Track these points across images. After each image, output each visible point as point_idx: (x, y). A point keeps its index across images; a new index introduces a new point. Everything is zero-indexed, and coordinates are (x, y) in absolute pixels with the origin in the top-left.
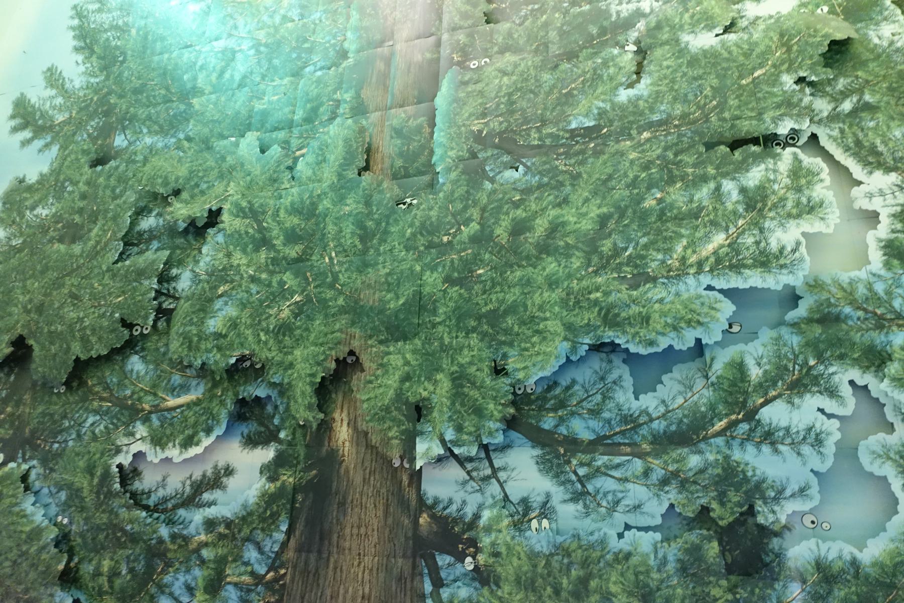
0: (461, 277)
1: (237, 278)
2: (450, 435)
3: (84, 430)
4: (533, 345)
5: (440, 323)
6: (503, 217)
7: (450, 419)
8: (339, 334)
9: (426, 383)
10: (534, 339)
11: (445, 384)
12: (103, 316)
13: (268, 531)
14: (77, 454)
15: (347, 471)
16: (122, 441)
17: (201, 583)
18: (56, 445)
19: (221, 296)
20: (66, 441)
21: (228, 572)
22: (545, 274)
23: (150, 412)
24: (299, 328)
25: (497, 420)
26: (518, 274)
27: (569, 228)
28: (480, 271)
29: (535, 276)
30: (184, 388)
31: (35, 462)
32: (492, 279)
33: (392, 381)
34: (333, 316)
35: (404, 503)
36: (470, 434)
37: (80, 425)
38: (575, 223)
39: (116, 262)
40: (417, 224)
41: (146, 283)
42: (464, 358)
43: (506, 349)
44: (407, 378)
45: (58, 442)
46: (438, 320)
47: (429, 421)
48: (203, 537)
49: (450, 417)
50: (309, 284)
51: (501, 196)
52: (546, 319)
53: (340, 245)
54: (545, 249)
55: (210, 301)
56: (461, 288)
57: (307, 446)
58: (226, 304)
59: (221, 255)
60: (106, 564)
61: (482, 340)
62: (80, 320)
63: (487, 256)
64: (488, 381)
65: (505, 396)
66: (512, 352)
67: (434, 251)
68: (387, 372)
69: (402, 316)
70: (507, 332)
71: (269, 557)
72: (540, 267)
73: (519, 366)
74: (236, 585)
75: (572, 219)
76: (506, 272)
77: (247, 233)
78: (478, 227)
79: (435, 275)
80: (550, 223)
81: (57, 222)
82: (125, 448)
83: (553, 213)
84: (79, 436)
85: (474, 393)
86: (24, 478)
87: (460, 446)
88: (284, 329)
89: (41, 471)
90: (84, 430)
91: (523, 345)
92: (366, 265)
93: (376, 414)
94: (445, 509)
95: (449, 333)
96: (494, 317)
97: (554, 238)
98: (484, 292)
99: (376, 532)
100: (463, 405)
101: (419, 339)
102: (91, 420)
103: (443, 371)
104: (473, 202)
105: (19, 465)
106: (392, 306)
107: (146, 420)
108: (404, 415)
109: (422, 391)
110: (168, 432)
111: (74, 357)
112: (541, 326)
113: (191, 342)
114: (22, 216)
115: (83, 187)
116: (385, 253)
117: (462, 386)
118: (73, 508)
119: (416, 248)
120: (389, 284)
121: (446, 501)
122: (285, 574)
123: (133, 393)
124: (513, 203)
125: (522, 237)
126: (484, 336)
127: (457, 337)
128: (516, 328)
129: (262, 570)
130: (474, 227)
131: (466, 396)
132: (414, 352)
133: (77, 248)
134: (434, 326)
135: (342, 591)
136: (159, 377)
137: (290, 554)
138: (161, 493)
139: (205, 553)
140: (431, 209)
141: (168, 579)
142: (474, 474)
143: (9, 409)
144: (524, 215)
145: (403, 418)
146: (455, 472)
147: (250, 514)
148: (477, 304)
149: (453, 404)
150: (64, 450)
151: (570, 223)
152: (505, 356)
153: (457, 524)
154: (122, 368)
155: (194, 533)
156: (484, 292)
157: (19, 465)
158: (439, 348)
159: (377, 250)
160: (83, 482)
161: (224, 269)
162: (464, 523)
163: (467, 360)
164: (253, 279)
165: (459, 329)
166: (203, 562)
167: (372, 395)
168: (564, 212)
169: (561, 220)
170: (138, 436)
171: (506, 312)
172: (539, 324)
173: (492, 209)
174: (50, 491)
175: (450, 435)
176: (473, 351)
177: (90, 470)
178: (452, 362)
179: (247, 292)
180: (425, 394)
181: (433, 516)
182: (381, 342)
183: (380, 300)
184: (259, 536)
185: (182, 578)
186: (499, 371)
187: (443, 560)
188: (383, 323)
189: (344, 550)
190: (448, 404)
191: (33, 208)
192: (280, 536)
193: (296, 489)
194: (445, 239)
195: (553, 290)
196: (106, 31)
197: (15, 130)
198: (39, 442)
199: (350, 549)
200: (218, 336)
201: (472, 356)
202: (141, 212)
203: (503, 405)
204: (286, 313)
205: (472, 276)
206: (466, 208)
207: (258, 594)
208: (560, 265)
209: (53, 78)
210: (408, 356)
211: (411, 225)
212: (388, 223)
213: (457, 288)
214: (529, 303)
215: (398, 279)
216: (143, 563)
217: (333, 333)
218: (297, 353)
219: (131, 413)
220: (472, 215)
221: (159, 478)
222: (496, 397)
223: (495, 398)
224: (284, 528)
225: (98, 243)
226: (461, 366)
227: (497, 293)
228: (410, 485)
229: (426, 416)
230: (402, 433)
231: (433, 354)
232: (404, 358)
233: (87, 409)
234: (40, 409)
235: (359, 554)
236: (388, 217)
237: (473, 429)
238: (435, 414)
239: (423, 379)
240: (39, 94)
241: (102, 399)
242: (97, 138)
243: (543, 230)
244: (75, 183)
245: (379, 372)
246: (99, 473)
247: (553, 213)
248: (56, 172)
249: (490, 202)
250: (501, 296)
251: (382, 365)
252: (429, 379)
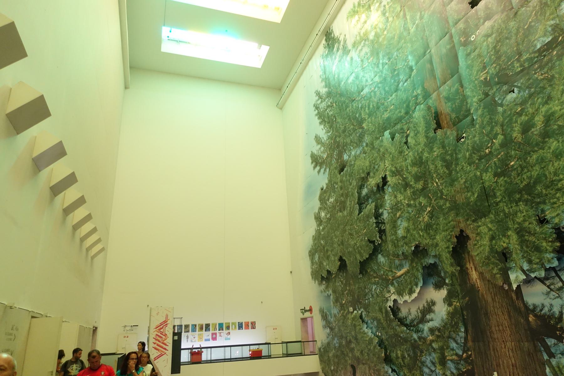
0: (503, 171)
1: (402, 207)
2: (526, 267)
4: (558, 199)
5: (500, 202)
6: (514, 125)
7: (523, 257)
8: (452, 223)
9: (503, 239)
10: (558, 195)
11: (514, 237)
12: (362, 240)
13: (457, 331)
14: (374, 304)
15: (483, 295)
16: (387, 295)
19: (399, 218)
21: (446, 354)
22: (551, 151)
23: (393, 280)
24: (434, 224)
25: (550, 252)
26: (535, 157)
27: (557, 115)
28: (512, 163)
29: (545, 155)
30: (401, 266)
31: (362, 310)
32: (521, 166)
33: (486, 241)
34: (447, 213)
35: (517, 310)
36: (537, 264)
38: (560, 110)
39: (359, 214)
40: (470, 148)
41: (371, 220)
42: (520, 219)
43: (542, 206)
44: (492, 238)
46: (498, 200)
47: (512, 260)
48: (431, 338)
49: (522, 256)
50: (431, 200)
51: (509, 112)
52: (561, 180)
53: (439, 174)
54: (546, 135)
55: (395, 222)
56: (504, 177)
57: (460, 285)
58: (402, 221)
59: (393, 198)
61: (526, 205)
62: (356, 244)
63: (513, 152)
64: (538, 229)
65: (551, 236)
66: (546, 207)
67: (483, 160)
68: (482, 237)
69: (479, 204)
70: (540, 195)
71: (461, 346)
72: (546, 148)
73: (554, 214)
74: (451, 360)
75: (557, 108)
76: (527, 158)
77: (399, 183)
78: (502, 137)
79: (489, 174)
80: (544, 117)
81: (337, 203)
82: (389, 298)
83: (544, 109)
84: (372, 295)
85: (532, 238)
86: (361, 317)
87: (534, 272)
88: (428, 226)
91: (552, 201)
92: (453, 181)
93: (484, 262)
94: (541, 310)
95: (507, 206)
96: (529, 188)
97: (550, 125)
98: (518, 175)
99: (508, 328)
100: (527, 247)
101: (492, 214)
102: (374, 288)
103: (510, 229)
104: (495, 123)
105: (358, 311)
106: (472, 199)
107: (392, 284)
108: (497, 260)
109: (503, 243)
110: (402, 288)
112: (559, 185)
113: (395, 243)
114: (326, 204)
115: (340, 184)
116: (460, 171)
117: (523, 236)
119: (474, 163)
120: (467, 188)
121: (541, 305)
122: (471, 354)
123: (384, 272)
124: (517, 113)
125: (530, 133)
126: (526, 201)
127: (512, 207)
128: (544, 191)
129: (461, 353)
130: (500, 137)
131: (528, 241)
132: (492, 222)
133: (345, 213)
134: (497, 204)
135: (501, 363)
136: (391, 262)
137: (470, 344)
139: (435, 345)
140: (474, 137)
142: (552, 287)
144: (527, 118)
145: (497, 262)
146: (540, 288)
147: (446, 324)
148: (517, 184)
149: (522, 247)
150: (369, 302)
151: (557, 111)
152: (543, 211)
153: (551, 319)
154: (377, 261)
155: (426, 335)
156: (518, 175)
157: (358, 311)
158: (504, 217)
159: (456, 170)
160: (379, 316)
161: (396, 204)
162: (556, 318)
163: (521, 219)
164: (409, 205)
165: (511, 202)
166: (435, 350)
167: (478, 252)
168: (551, 106)
169: (550, 112)
170: (392, 292)
171: (535, 183)
172: (557, 185)
173: (507, 122)
175: (526, 267)
176: (523, 213)
177: (380, 310)
178: (514, 223)
179: (408, 212)
180: (505, 245)
181: (535, 316)
182: (474, 221)
183: (466, 198)
184: (454, 335)
186: (542, 221)
187: (551, 342)
188: (470, 210)
189: (495, 339)
190: (519, 248)
191: (328, 200)
192: (462, 335)
193: (462, 309)
194: (487, 151)
195: (560, 160)
196: (326, 110)
197: (315, 168)
199: (498, 339)
200: (404, 238)
201: (524, 216)
202: (361, 187)
203: (551, 242)
204: (426, 218)
205: (509, 168)
206: (492, 129)
207: (462, 365)
208: (559, 142)
209: (318, 140)
210: (489, 225)
211: (468, 150)
212: (456, 154)
213: (502, 178)
214: (547, 173)
215: (471, 183)
217: (450, 222)
218: (438, 237)
219: (386, 282)
220: (497, 131)
221: (408, 311)
222: (545, 238)
223: (545, 239)
224: (463, 330)
225: (350, 208)
226: (519, 224)
227: (525, 173)
228: (517, 299)
229: (510, 258)
230: (500, 270)
231: (501, 221)
232: (488, 227)
235: (503, 341)
236: (455, 150)
237: (538, 261)
238: (514, 256)
239: (501, 237)
240: (316, 149)
241: (375, 277)
242: (338, 159)
243: (541, 123)
244: (337, 184)
245: (478, 238)
247: (544, 109)
248: (330, 181)
249: (504, 119)
250: (528, 174)
251: (478, 234)
252: (504, 236)
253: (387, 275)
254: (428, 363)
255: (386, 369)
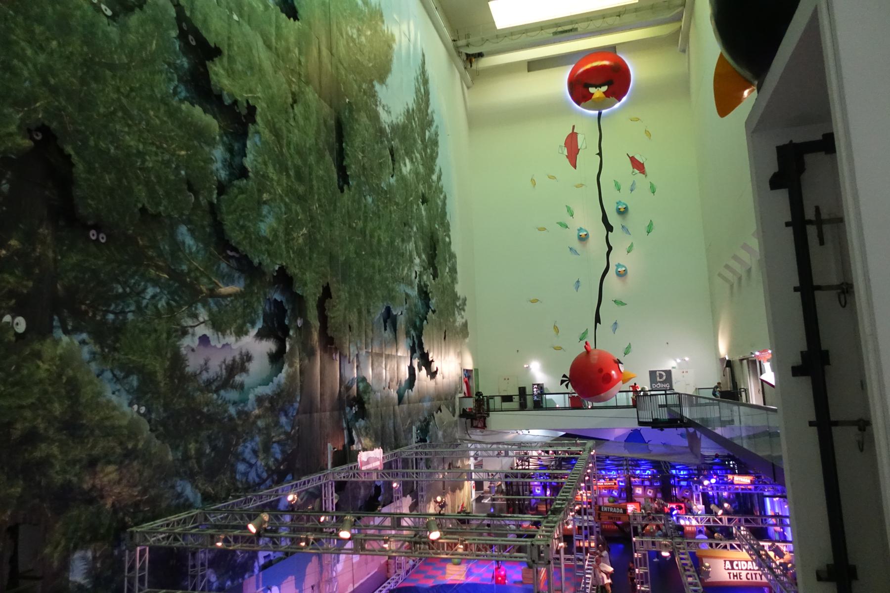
3: (145, 302)
12: (167, 164)
14: (142, 331)
16: (188, 322)
17: (260, 446)
18: (111, 317)
20: (123, 312)
21: (273, 434)
30: (230, 280)
37: (139, 294)
45: (112, 312)
48: (257, 412)
60: (192, 446)
74: (278, 442)
82: (190, 330)
89: (97, 349)
90: (145, 302)
107: (205, 304)
111: (140, 205)
118: (149, 395)
123: (190, 271)
138: (205, 376)
141: (240, 449)
143: (13, 242)
147: (282, 391)
155: (251, 408)
170: (201, 319)
174: (114, 375)
185: (249, 445)
198: (83, 307)
216: (222, 439)
221: (202, 362)
233: (143, 276)
234: (74, 258)
241: (158, 268)
246: (169, 355)
253: (197, 279)
254: (248, 455)
255: (179, 489)
